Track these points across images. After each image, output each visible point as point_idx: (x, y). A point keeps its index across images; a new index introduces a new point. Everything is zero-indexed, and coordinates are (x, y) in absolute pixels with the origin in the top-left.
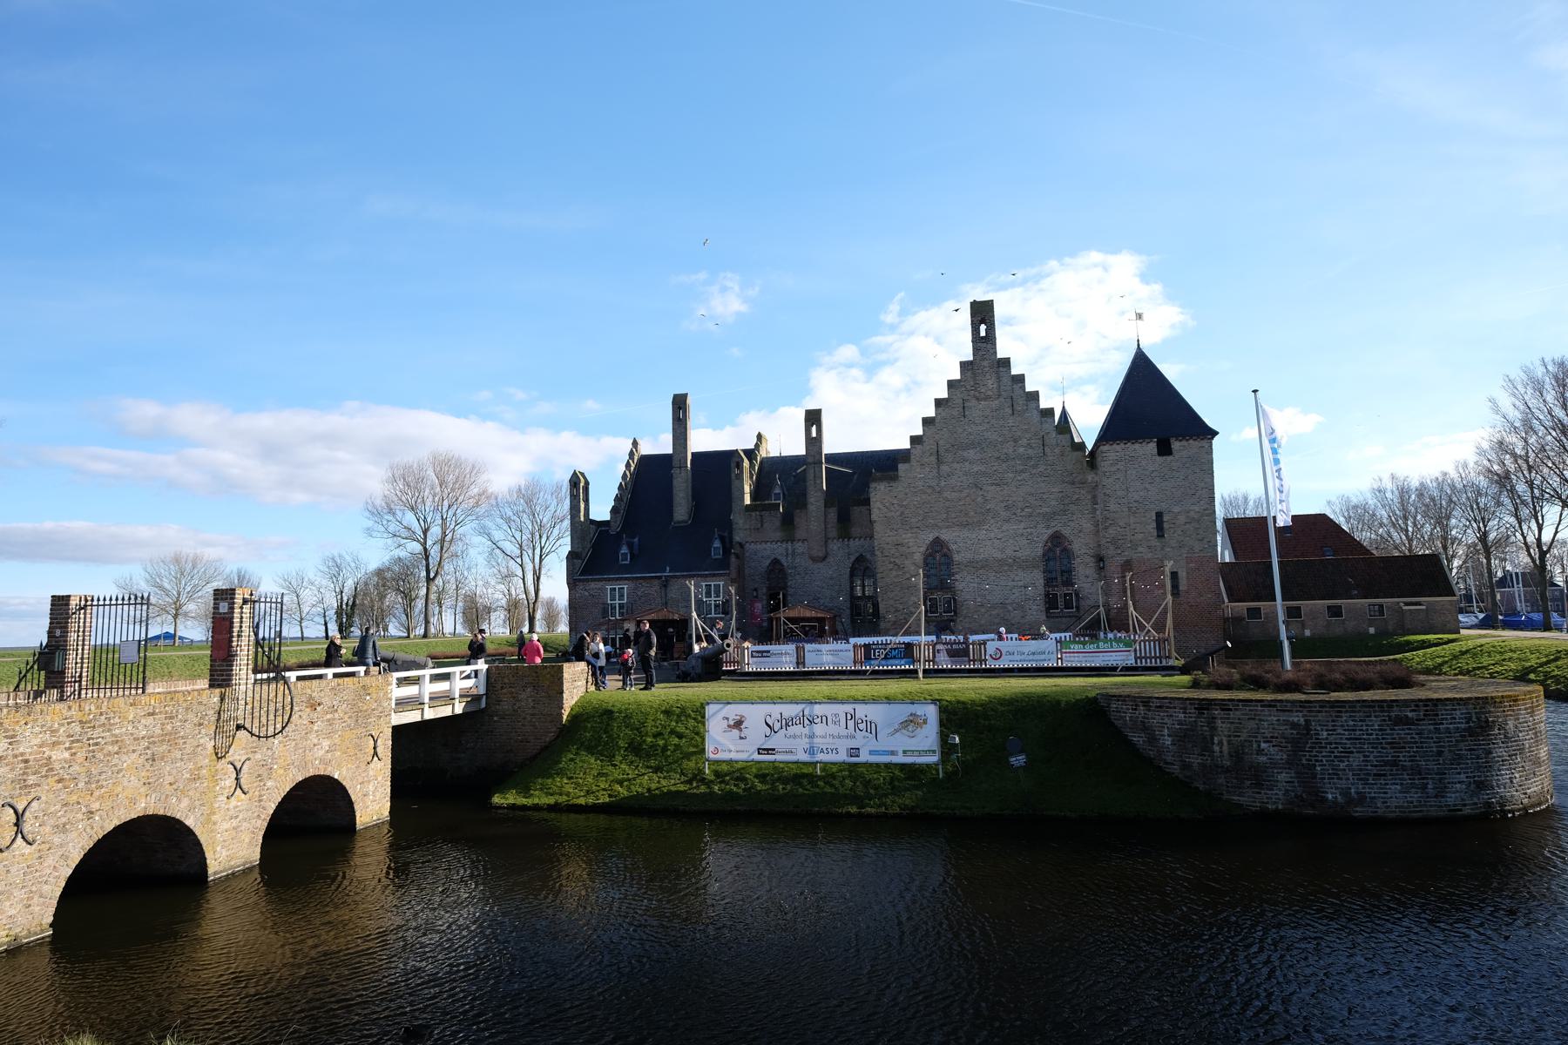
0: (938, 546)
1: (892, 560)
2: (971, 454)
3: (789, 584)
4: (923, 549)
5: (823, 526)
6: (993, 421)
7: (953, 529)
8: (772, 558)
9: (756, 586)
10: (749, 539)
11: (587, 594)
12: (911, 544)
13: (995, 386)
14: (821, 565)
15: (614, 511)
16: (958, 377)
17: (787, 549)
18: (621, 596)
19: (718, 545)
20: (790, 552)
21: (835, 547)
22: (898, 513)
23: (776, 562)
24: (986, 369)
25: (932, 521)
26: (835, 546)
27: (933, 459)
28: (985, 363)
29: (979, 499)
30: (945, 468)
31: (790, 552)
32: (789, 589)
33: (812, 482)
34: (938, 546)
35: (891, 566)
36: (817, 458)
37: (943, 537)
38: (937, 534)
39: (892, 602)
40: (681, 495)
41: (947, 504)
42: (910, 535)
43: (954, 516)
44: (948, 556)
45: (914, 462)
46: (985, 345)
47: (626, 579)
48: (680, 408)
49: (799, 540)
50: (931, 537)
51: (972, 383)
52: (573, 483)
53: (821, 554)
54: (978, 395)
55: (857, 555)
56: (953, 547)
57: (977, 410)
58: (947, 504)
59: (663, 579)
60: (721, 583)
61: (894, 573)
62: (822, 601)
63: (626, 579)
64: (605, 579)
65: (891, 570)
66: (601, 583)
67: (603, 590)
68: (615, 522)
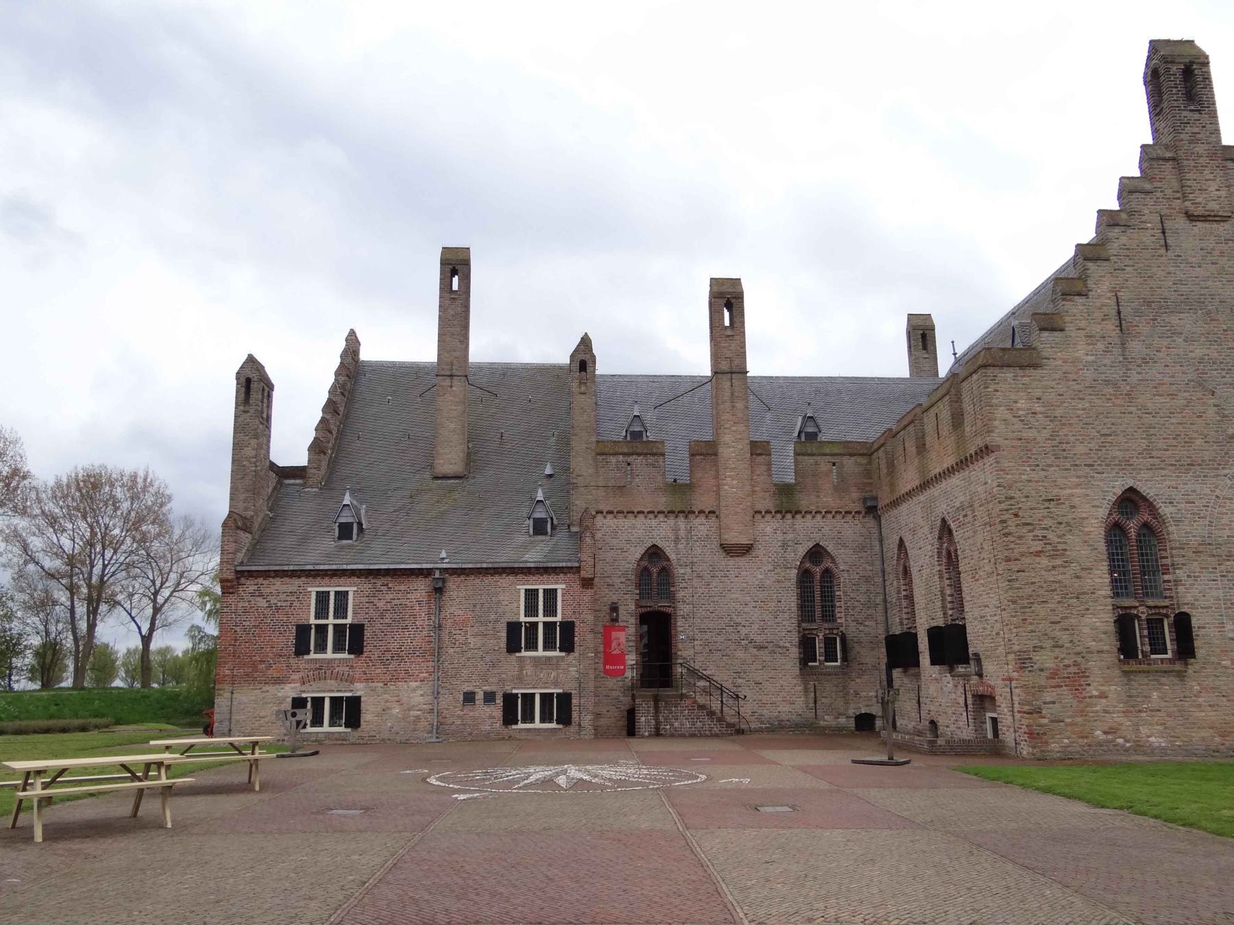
0: (1130, 500)
1: (1039, 533)
2: (1185, 322)
3: (680, 595)
4: (1103, 512)
5: (748, 488)
6: (1223, 261)
7: (1164, 472)
8: (649, 544)
9: (614, 598)
10: (604, 507)
11: (262, 603)
12: (1076, 501)
13: (1223, 193)
14: (742, 561)
15: (316, 448)
16: (1136, 173)
17: (676, 530)
18: (341, 611)
19: (543, 515)
20: (682, 533)
21: (769, 529)
22: (1046, 433)
23: (654, 553)
24: (1201, 160)
25: (1118, 453)
26: (768, 527)
27: (1111, 326)
28: (1200, 149)
29: (1211, 412)
30: (1135, 347)
31: (682, 533)
32: (680, 605)
33: (728, 404)
34: (1130, 500)
35: (1038, 546)
36: (737, 362)
37: (1143, 489)
38: (1130, 483)
39: (1044, 626)
40: (452, 426)
41: (1148, 420)
42: (1074, 480)
43: (1161, 445)
44: (1151, 532)
45: (1070, 328)
46: (1197, 116)
48: (454, 272)
49: (701, 512)
50: (1118, 487)
51: (1176, 185)
52: (243, 380)
53: (744, 540)
54: (1192, 208)
55: (811, 545)
56: (1166, 510)
57: (1189, 238)
58: (1148, 420)
59: (437, 575)
60: (560, 587)
61: (1044, 561)
62: (744, 631)
65: (1038, 554)
66: (294, 584)
67: (301, 595)
68: (318, 468)
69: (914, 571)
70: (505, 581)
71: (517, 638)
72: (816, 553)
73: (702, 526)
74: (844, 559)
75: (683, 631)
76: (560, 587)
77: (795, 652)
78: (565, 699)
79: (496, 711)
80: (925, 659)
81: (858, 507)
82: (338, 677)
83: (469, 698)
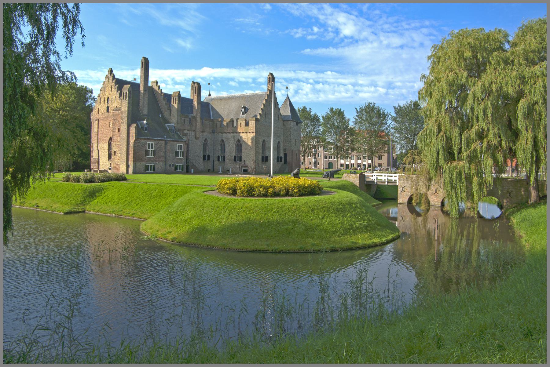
47: (155, 140)
60: (182, 145)
63: (155, 140)
64: (147, 139)
69: (226, 146)
70: (175, 143)
71: (177, 153)
72: (206, 140)
73: (193, 133)
74: (209, 140)
75: (190, 152)
76: (182, 145)
77: (202, 158)
78: (183, 166)
79: (173, 168)
80: (227, 161)
81: (211, 131)
82: (152, 161)
83: (170, 165)
